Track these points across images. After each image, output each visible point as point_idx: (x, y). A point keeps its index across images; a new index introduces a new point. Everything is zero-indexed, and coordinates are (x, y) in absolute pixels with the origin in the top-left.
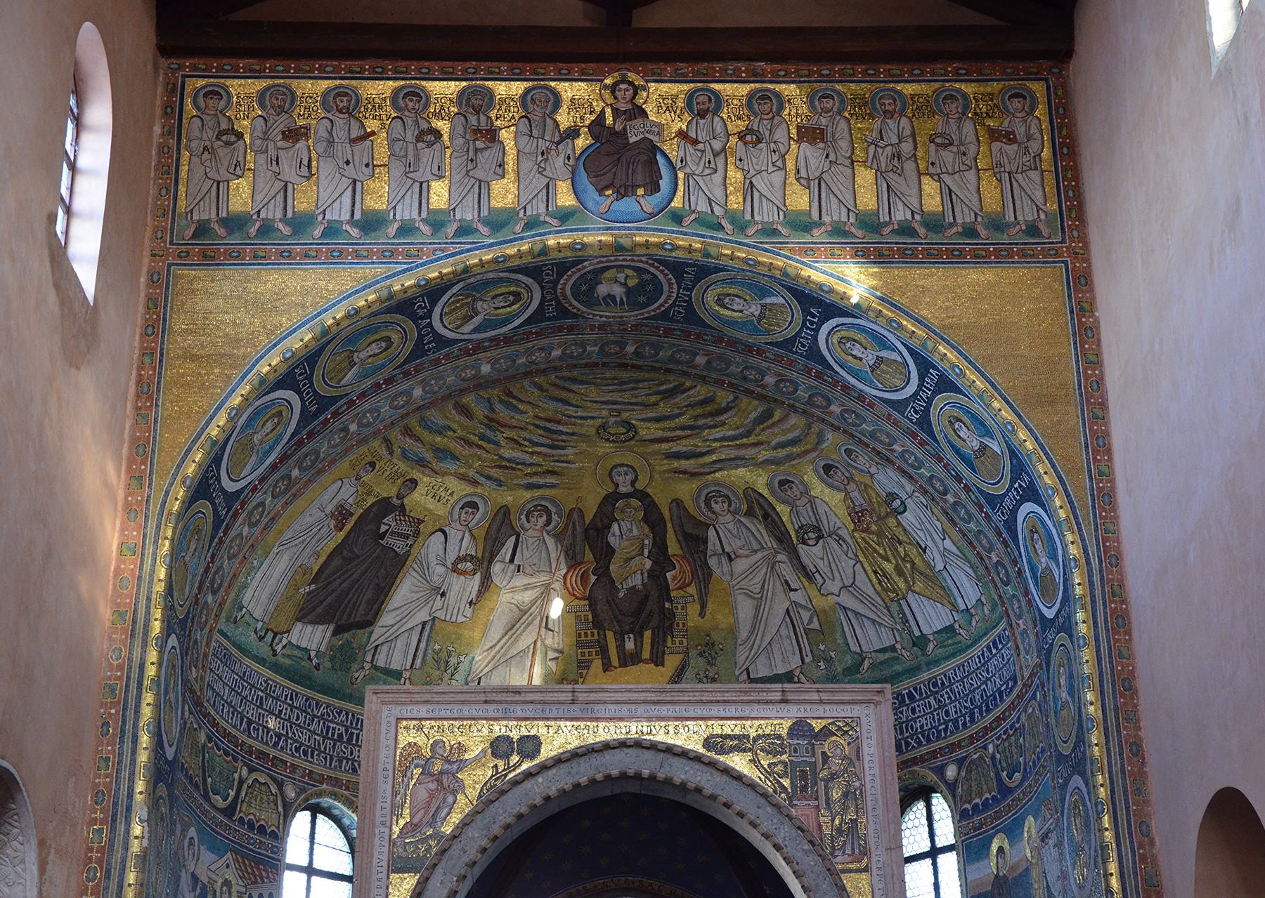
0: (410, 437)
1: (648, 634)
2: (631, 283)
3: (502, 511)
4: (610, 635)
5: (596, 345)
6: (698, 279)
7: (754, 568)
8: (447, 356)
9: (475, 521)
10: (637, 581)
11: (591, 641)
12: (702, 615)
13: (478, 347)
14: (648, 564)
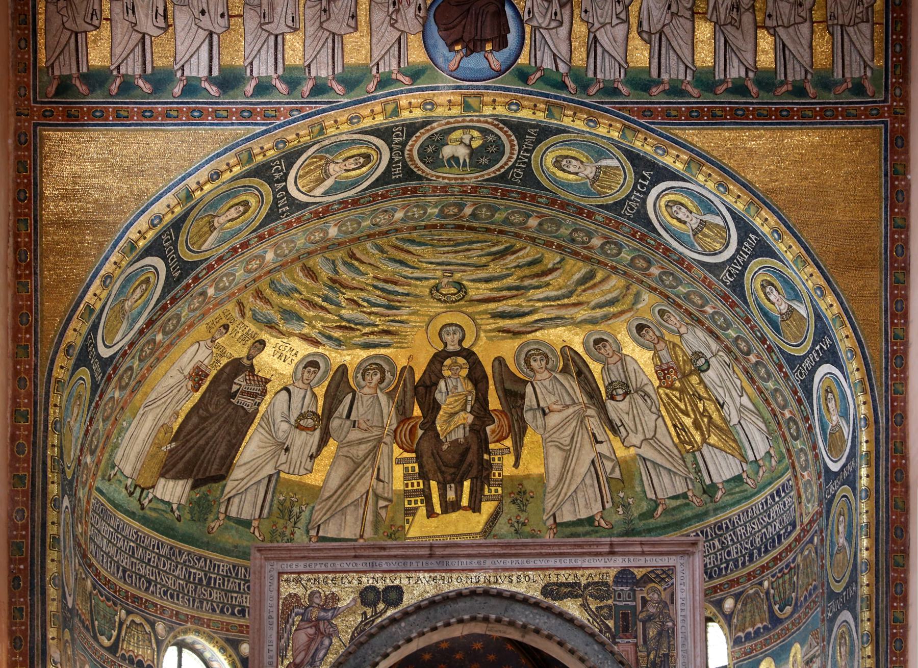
0: (261, 299)
1: (467, 484)
2: (476, 144)
3: (341, 370)
4: (433, 484)
5: (436, 207)
6: (539, 141)
7: (565, 422)
8: (298, 220)
9: (316, 379)
10: (459, 435)
11: (417, 490)
12: (516, 465)
13: (327, 211)
14: (470, 418)
